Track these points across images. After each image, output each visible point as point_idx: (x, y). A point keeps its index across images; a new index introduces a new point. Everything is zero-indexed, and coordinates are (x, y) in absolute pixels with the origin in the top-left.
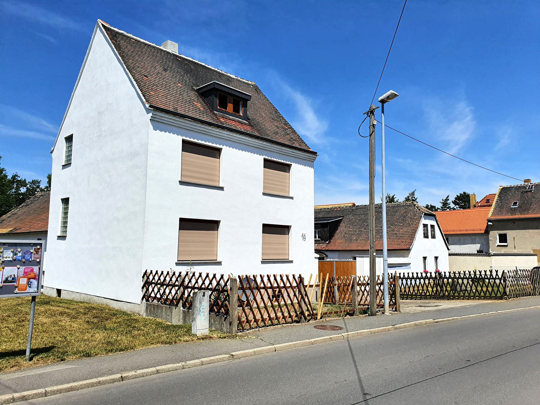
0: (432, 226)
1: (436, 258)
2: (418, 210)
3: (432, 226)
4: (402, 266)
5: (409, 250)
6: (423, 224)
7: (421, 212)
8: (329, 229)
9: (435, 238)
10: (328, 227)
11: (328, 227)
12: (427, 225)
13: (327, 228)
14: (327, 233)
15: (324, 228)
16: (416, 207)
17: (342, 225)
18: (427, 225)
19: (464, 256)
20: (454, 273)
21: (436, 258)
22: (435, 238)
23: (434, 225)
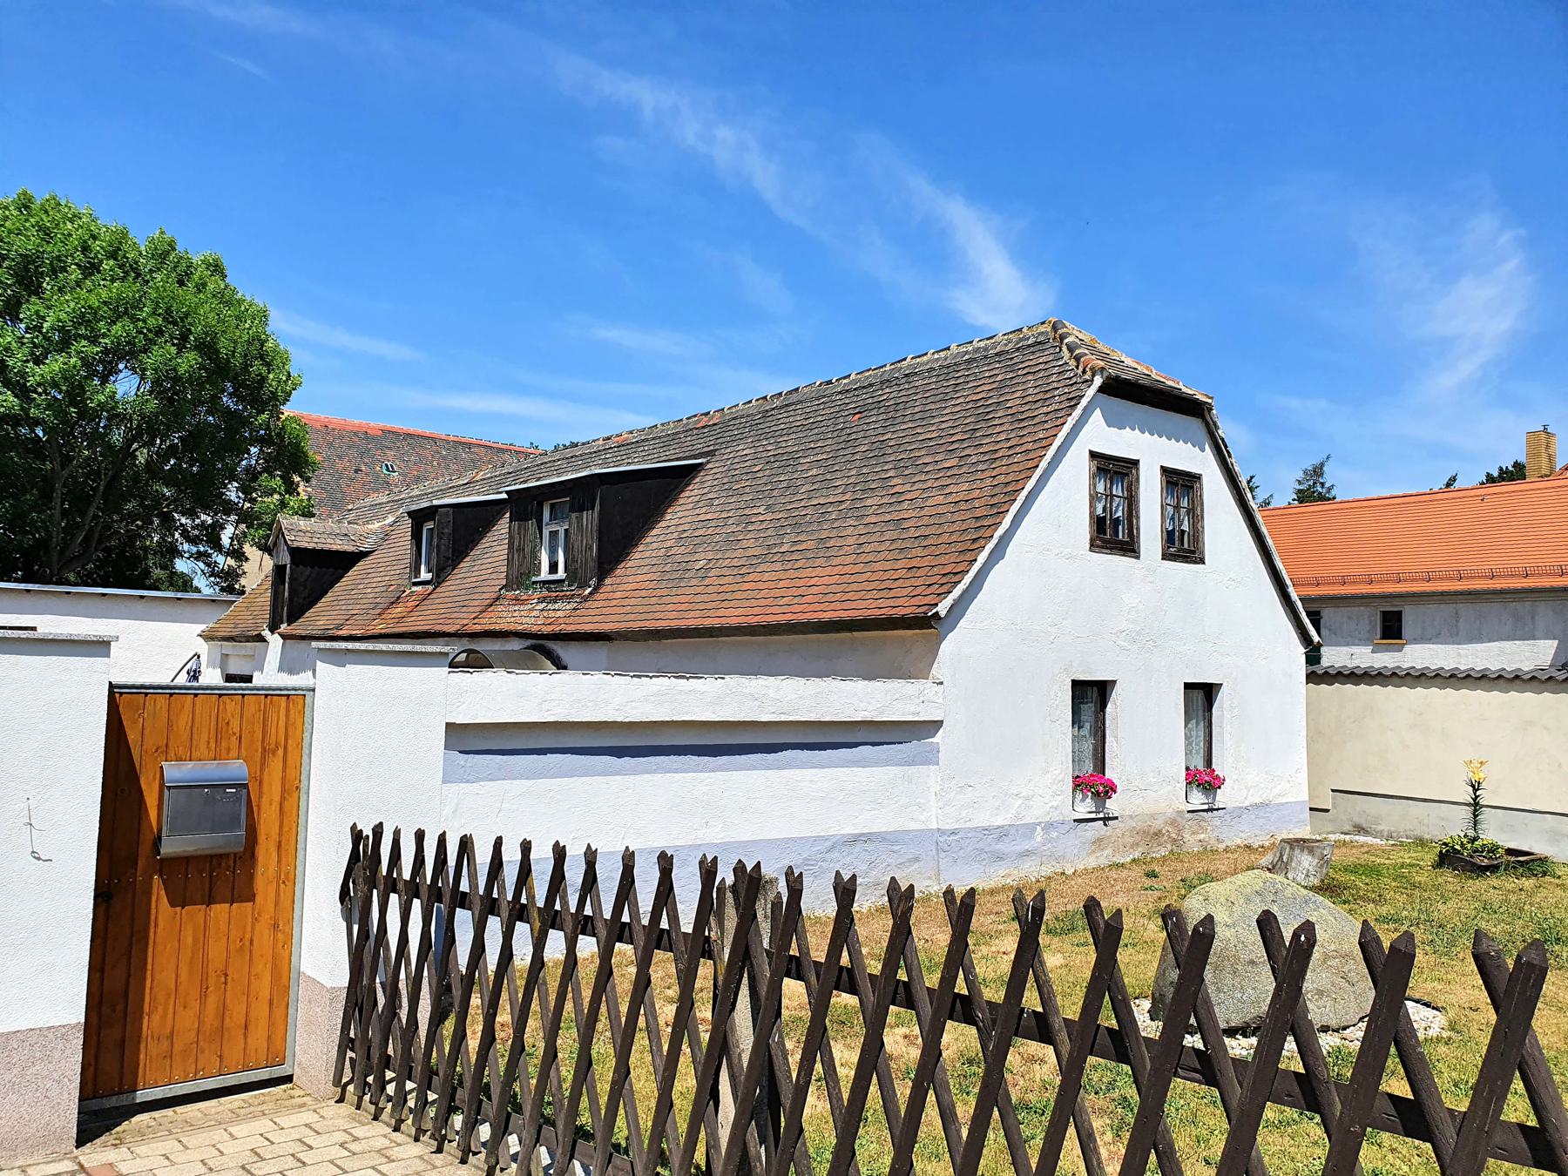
0: (1180, 483)
1: (1202, 696)
2: (1073, 363)
3: (1180, 483)
4: (856, 745)
5: (928, 625)
6: (1094, 455)
7: (1084, 372)
8: (600, 513)
9: (1202, 561)
10: (597, 508)
11: (597, 508)
12: (1135, 463)
13: (593, 509)
14: (592, 538)
15: (581, 510)
16: (1064, 348)
17: (691, 493)
18: (1135, 463)
19: (1318, 684)
20: (901, 900)
21: (1202, 696)
22: (1202, 561)
23: (1197, 478)
